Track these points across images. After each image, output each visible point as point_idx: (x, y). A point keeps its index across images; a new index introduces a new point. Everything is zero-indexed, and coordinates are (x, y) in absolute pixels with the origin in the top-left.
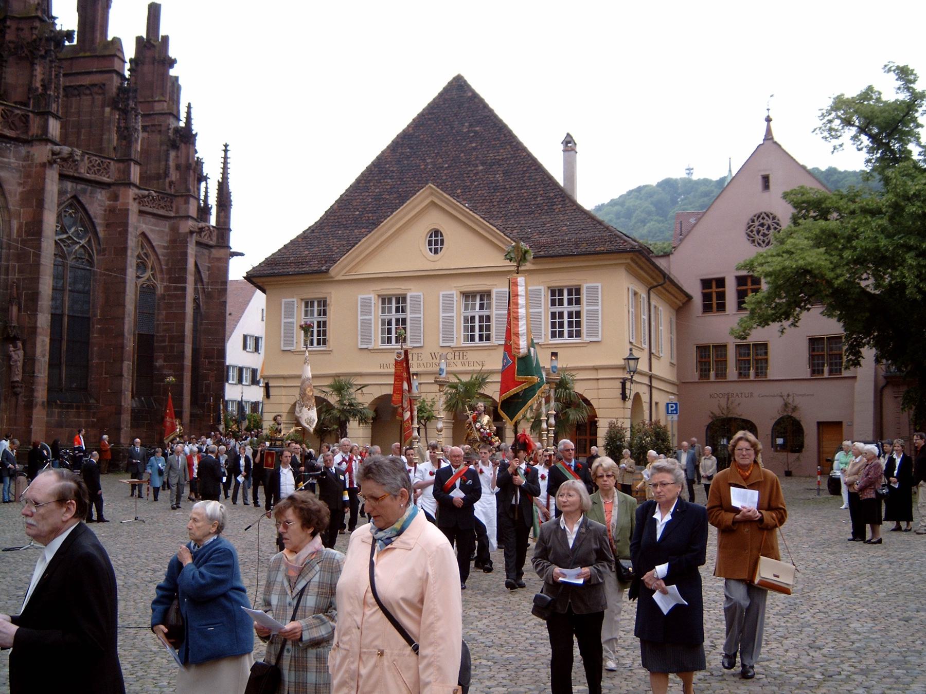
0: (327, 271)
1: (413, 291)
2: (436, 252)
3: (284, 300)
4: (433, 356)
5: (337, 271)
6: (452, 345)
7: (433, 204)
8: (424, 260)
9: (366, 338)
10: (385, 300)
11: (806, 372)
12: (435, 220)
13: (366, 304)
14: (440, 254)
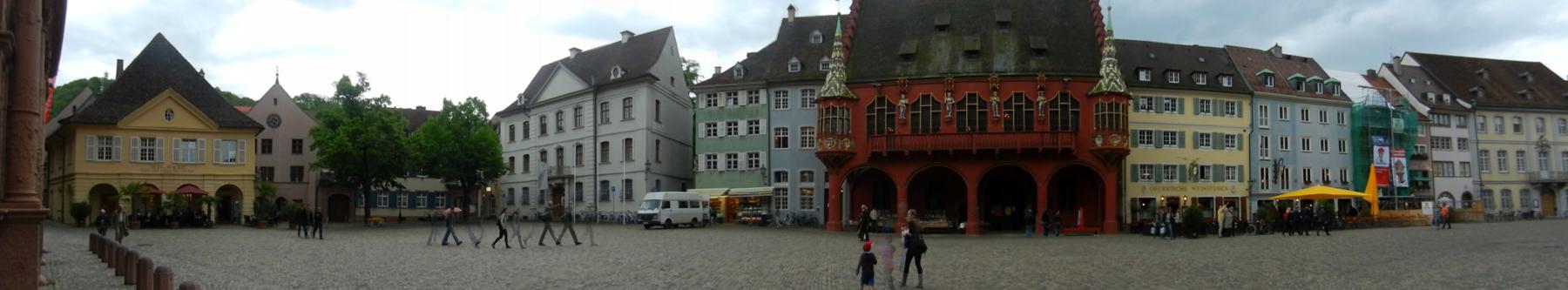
0: (115, 124)
1: (159, 137)
2: (169, 119)
3: (88, 136)
4: (169, 167)
5: (121, 124)
6: (179, 162)
7: (170, 97)
8: (164, 124)
9: (135, 158)
10: (144, 140)
11: (289, 180)
12: (170, 105)
13: (135, 142)
14: (172, 121)
